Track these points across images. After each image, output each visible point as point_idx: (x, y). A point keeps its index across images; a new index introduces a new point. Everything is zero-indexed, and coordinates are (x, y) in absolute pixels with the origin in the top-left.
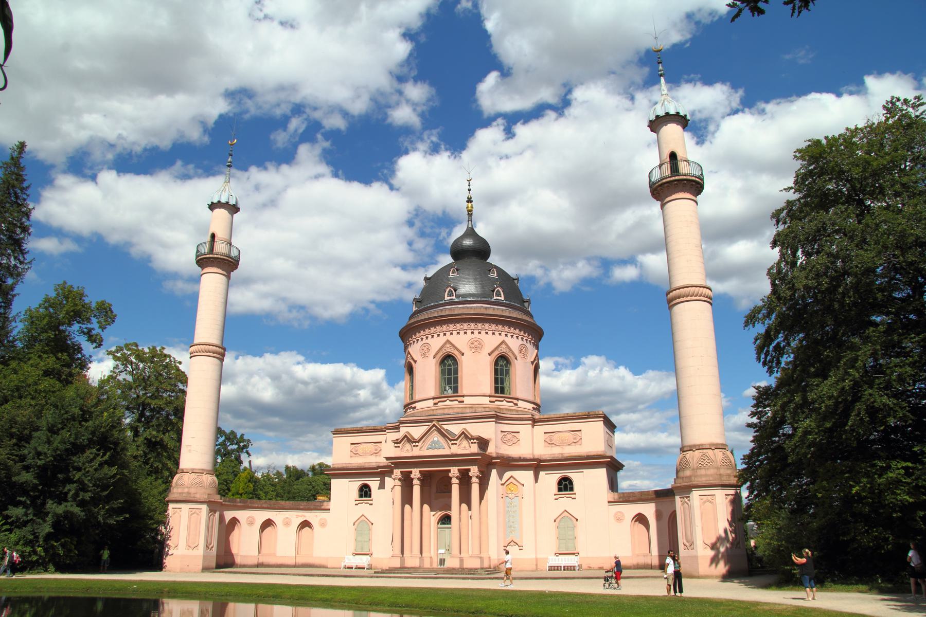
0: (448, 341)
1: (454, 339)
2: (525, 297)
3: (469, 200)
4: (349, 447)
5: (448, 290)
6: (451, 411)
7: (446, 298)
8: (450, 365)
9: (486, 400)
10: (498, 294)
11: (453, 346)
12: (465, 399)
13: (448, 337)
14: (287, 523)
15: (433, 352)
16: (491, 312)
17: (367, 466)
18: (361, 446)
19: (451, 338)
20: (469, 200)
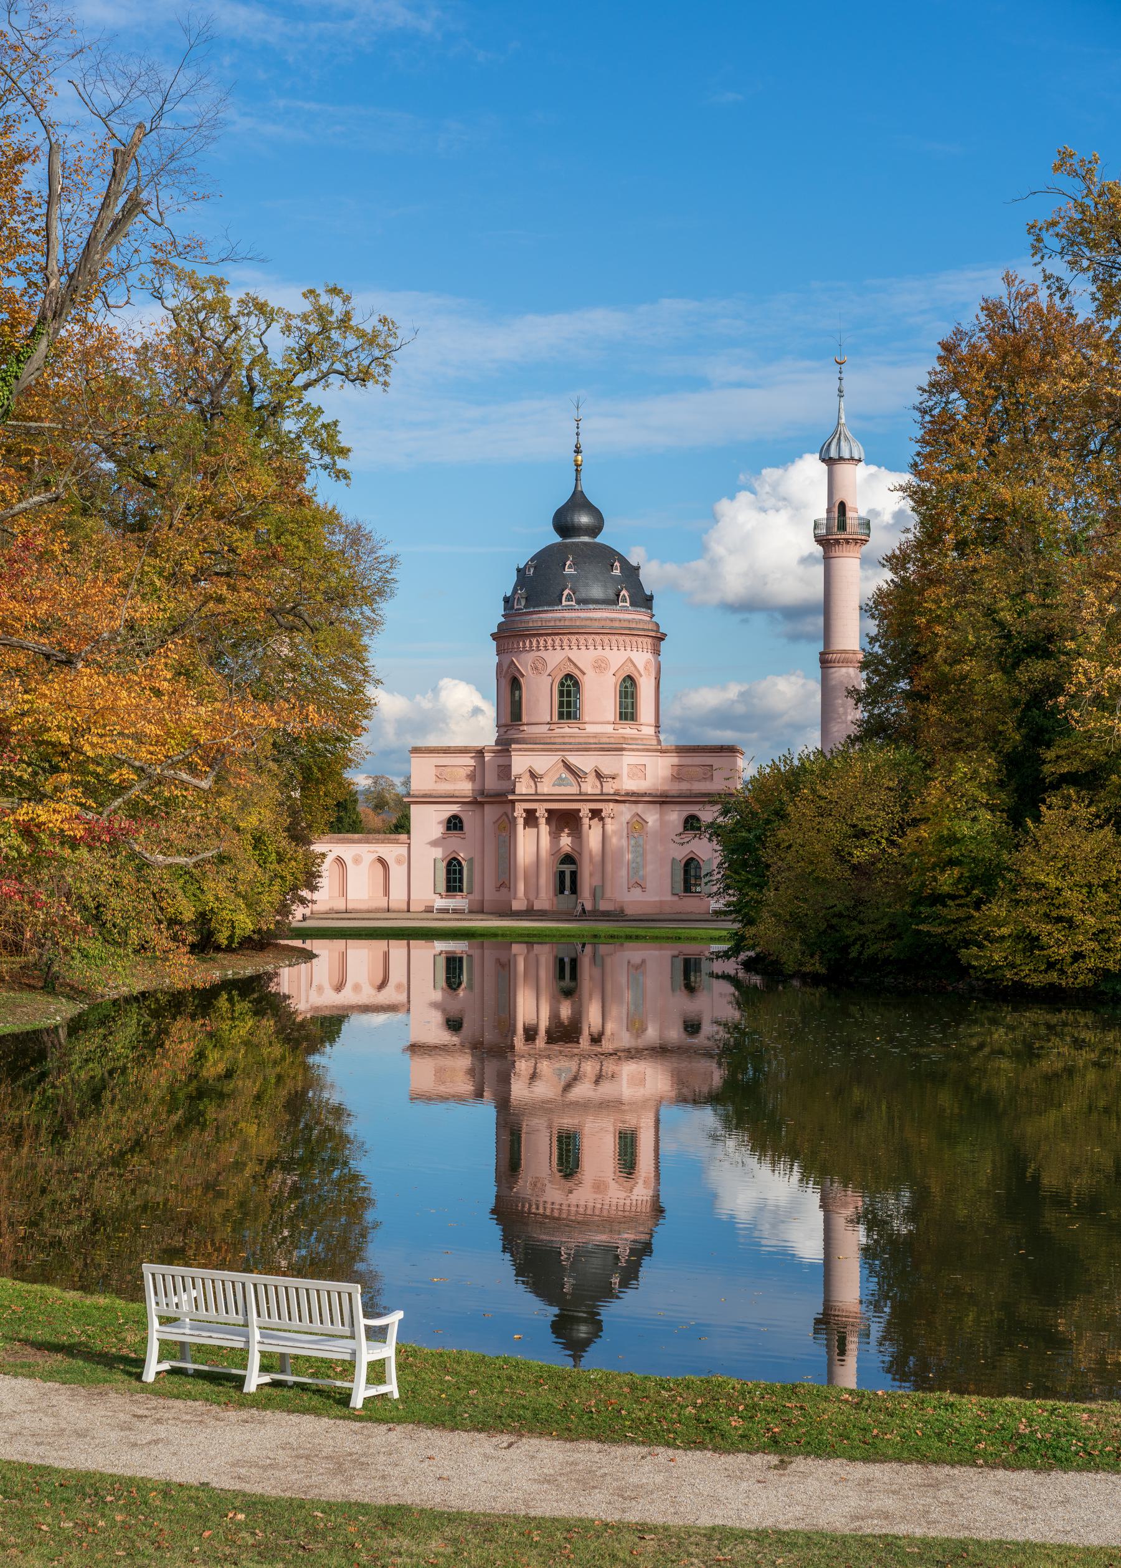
0: (570, 660)
1: (574, 655)
2: (648, 593)
3: (578, 451)
4: (434, 771)
5: (566, 592)
6: (572, 740)
7: (564, 603)
8: (568, 686)
9: (609, 729)
10: (624, 600)
11: (575, 665)
12: (586, 726)
13: (567, 652)
14: (357, 860)
15: (548, 672)
16: (617, 624)
17: (457, 793)
18: (448, 770)
19: (574, 655)
20: (578, 451)
